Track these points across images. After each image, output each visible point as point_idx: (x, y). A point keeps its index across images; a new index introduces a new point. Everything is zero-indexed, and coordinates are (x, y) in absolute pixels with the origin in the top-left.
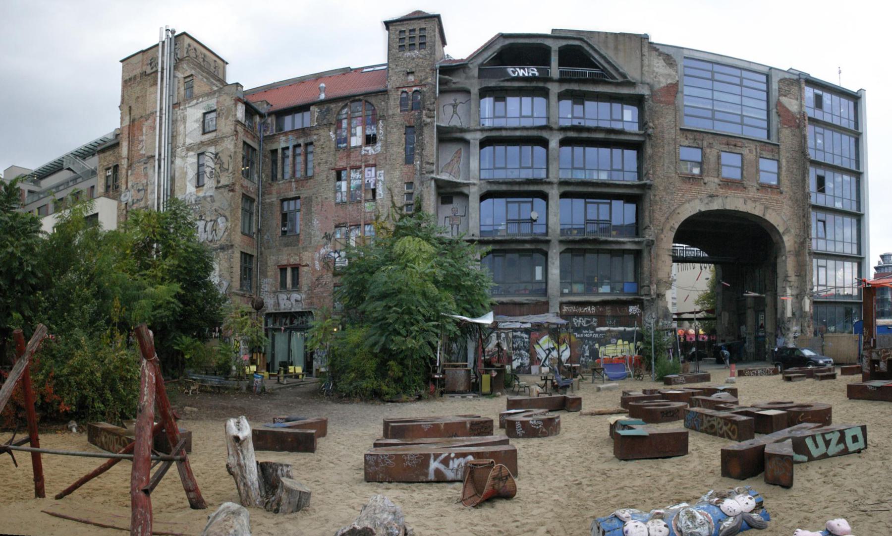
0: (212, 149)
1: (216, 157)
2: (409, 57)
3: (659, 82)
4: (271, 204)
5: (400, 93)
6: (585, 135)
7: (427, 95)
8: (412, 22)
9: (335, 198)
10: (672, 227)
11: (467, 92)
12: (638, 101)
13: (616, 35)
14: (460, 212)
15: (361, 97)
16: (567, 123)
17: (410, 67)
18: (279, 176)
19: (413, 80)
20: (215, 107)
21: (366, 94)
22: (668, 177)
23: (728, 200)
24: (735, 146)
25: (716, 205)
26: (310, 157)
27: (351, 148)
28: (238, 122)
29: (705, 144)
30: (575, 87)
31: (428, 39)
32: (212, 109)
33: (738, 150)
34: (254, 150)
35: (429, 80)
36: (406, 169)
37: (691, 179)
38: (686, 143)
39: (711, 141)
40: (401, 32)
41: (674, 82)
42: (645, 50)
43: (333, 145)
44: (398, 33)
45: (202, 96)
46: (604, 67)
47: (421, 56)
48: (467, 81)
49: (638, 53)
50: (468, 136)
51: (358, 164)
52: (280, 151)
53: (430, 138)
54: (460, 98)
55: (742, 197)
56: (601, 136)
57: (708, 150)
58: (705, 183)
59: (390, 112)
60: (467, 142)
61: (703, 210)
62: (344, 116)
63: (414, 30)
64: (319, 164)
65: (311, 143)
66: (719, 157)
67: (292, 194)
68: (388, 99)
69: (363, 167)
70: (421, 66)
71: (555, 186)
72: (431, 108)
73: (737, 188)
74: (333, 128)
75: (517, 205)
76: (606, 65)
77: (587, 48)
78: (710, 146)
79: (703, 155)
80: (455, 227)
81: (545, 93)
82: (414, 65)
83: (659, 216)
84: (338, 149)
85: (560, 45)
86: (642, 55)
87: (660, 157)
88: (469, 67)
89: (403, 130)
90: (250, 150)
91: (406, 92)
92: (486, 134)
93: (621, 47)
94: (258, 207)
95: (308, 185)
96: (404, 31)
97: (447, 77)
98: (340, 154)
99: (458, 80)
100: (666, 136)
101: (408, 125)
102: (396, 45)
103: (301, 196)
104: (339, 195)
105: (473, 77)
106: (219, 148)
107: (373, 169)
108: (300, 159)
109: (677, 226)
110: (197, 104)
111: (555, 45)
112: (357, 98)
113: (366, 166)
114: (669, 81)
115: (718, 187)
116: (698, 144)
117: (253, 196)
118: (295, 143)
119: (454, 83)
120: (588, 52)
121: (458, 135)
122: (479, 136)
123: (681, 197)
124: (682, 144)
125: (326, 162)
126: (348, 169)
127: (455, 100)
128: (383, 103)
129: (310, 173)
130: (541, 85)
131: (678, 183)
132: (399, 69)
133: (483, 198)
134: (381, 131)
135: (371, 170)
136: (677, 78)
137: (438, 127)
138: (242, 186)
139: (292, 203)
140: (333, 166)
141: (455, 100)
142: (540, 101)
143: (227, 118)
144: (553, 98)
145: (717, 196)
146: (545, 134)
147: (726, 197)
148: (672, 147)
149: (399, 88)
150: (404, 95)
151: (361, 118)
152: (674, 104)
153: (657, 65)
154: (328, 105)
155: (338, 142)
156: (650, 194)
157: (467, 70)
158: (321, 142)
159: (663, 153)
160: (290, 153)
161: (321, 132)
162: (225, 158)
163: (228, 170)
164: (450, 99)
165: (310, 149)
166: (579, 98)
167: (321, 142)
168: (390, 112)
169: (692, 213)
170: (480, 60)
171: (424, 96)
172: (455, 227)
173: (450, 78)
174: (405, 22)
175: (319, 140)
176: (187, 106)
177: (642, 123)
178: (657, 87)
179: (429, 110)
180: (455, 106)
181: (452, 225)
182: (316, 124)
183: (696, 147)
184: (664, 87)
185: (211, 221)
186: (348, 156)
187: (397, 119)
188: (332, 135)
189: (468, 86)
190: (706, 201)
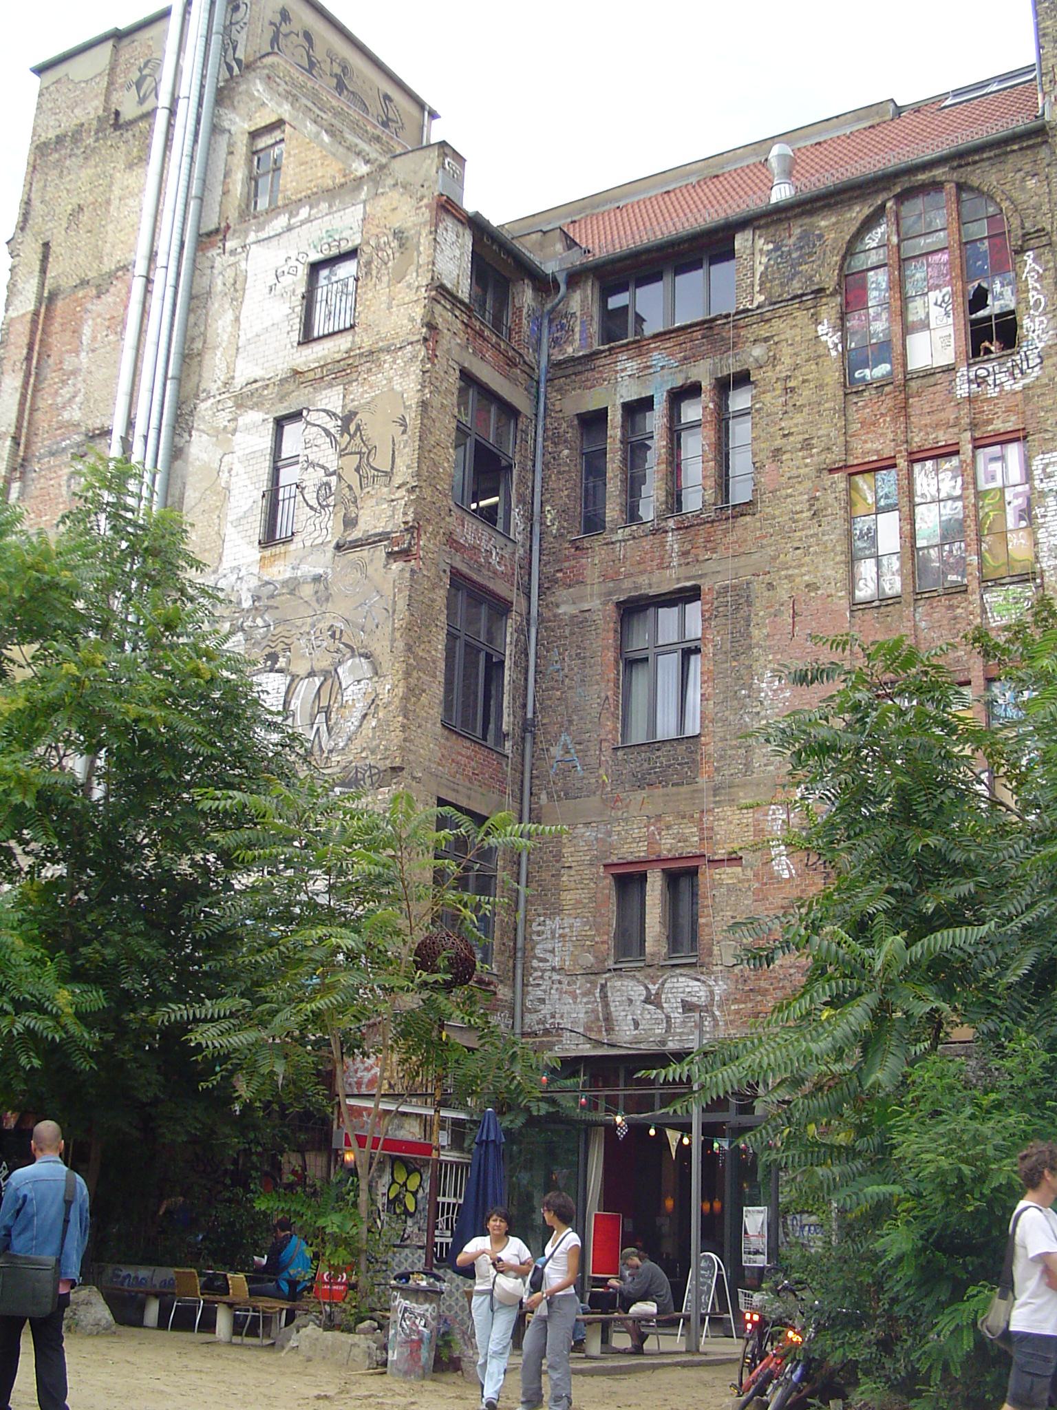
0: (332, 399)
1: (344, 429)
4: (581, 622)
9: (852, 581)
15: (939, 173)
18: (612, 511)
21: (961, 157)
26: (741, 431)
27: (908, 377)
28: (441, 292)
32: (346, 247)
34: (509, 412)
43: (833, 376)
45: (311, 199)
51: (943, 438)
52: (615, 418)
62: (874, 258)
65: (743, 379)
74: (829, 310)
84: (851, 388)
94: (523, 631)
95: (731, 538)
98: (863, 408)
103: (705, 588)
104: (867, 568)
106: (360, 394)
107: (1014, 452)
108: (695, 447)
110: (289, 229)
112: (922, 177)
113: (978, 445)
117: (500, 588)
118: (679, 382)
125: (807, 445)
126: (902, 463)
128: (1031, 183)
129: (740, 493)
134: (1033, 296)
135: (1002, 458)
138: (451, 541)
140: (836, 456)
151: (944, 257)
154: (807, 220)
155: (851, 361)
158: (782, 369)
160: (656, 421)
162: (379, 430)
163: (389, 474)
165: (740, 400)
167: (782, 369)
175: (774, 360)
176: (252, 237)
185: (311, 674)
186: (904, 409)
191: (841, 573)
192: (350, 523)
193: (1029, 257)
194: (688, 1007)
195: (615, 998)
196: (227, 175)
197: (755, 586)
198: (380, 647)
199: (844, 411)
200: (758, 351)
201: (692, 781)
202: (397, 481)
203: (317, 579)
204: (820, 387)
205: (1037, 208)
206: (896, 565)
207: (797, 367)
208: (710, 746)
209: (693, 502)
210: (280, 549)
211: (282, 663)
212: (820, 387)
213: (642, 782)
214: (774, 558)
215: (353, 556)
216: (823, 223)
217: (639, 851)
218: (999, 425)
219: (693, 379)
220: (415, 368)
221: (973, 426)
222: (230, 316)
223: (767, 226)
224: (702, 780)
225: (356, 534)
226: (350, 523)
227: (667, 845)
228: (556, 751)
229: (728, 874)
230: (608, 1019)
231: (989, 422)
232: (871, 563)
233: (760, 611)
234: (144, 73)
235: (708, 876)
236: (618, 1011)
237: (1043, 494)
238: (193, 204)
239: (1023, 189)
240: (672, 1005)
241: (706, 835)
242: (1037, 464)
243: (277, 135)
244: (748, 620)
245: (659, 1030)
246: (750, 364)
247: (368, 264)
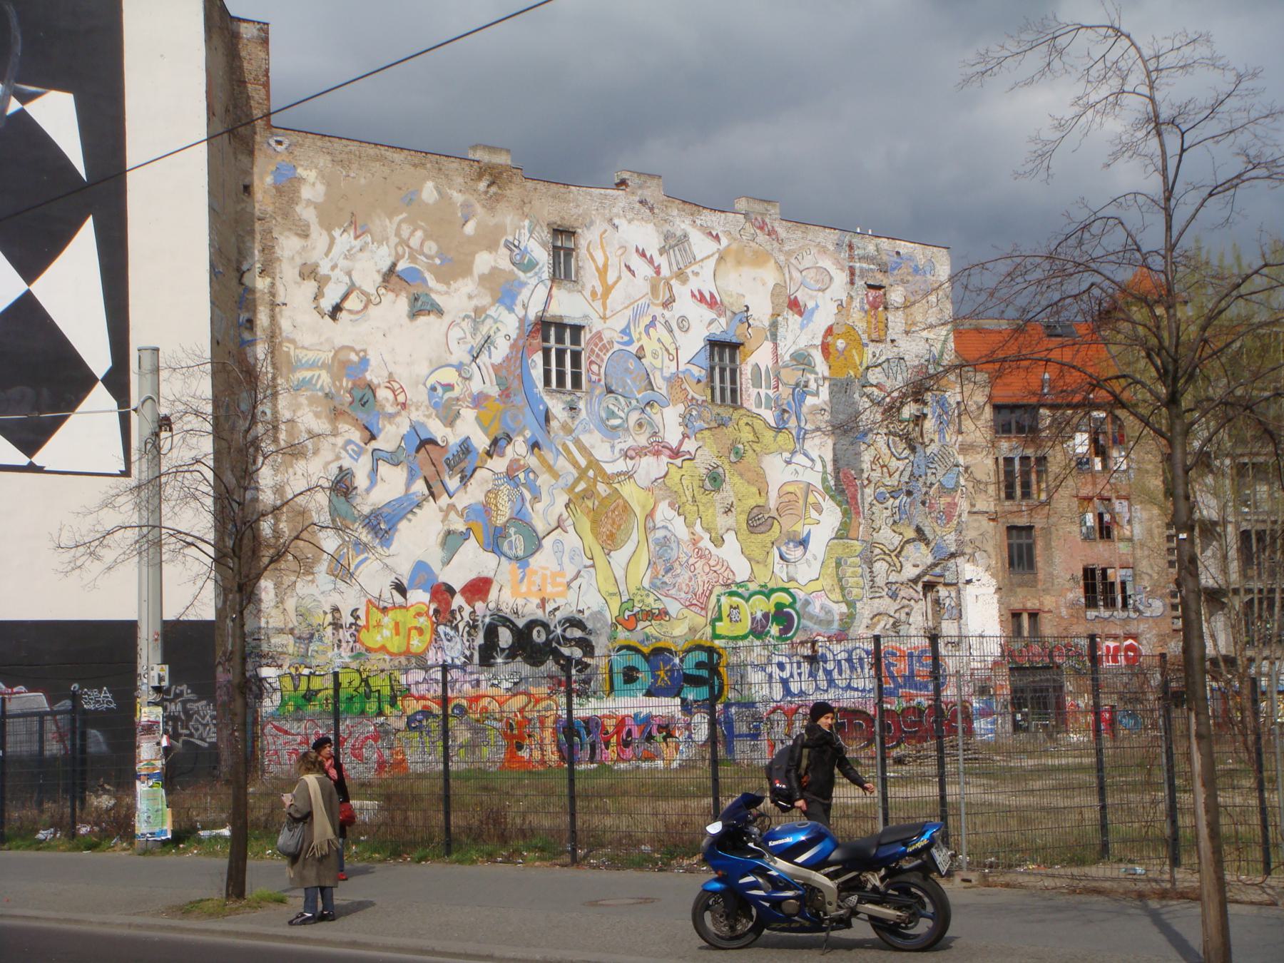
192: (973, 505)
198: (990, 549)
215: (975, 517)
224: (1039, 587)
225: (975, 510)
226: (973, 505)
227: (1029, 605)
233: (1054, 537)
235: (1042, 615)
241: (1042, 603)
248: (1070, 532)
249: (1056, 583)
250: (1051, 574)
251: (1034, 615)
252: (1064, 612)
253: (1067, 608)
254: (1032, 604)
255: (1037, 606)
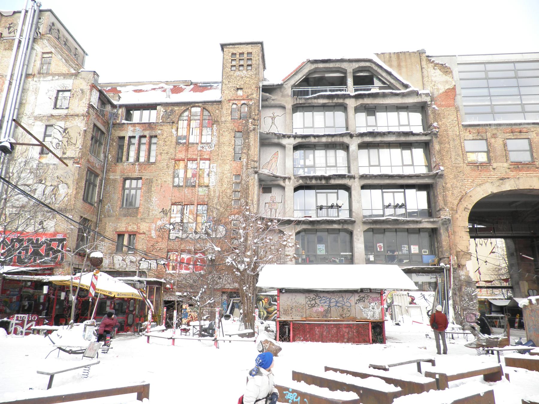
2: (239, 76)
3: (438, 89)
4: (115, 180)
5: (231, 105)
6: (378, 139)
7: (253, 107)
8: (242, 46)
9: (173, 182)
10: (465, 208)
11: (284, 107)
12: (422, 108)
13: (398, 54)
14: (278, 199)
15: (200, 104)
16: (363, 130)
17: (240, 84)
18: (124, 158)
19: (241, 95)
20: (70, 88)
22: (457, 167)
23: (521, 180)
24: (520, 132)
25: (508, 186)
26: (153, 147)
29: (489, 135)
30: (367, 101)
31: (254, 62)
33: (523, 135)
34: (103, 133)
35: (254, 96)
36: (234, 164)
37: (477, 166)
38: (471, 136)
39: (495, 132)
40: (233, 54)
41: (451, 87)
42: (424, 63)
44: (230, 54)
46: (390, 82)
47: (248, 76)
48: (283, 99)
49: (419, 67)
50: (284, 141)
51: (194, 157)
52: (127, 139)
53: (254, 141)
54: (278, 112)
55: (535, 176)
56: (392, 139)
57: (493, 140)
58: (494, 169)
59: (223, 119)
60: (283, 147)
61: (495, 191)
63: (243, 53)
64: (161, 154)
65: (156, 136)
66: (505, 145)
67: (136, 175)
68: (222, 109)
69: (199, 160)
70: (248, 84)
71: (357, 180)
72: (256, 118)
73: (528, 169)
75: (325, 194)
76: (392, 81)
77: (376, 68)
78: (494, 136)
79: (489, 145)
80: (273, 210)
81: (344, 108)
82: (243, 83)
83: (452, 200)
84: (178, 143)
85: (354, 68)
86: (422, 68)
87: (447, 151)
88: (284, 87)
89: (233, 134)
90: (99, 132)
91: (236, 104)
92: (299, 140)
93: (403, 64)
95: (150, 169)
96: (235, 54)
97: (267, 94)
98: (179, 148)
99: (276, 98)
100: (450, 133)
101: (237, 130)
102: (229, 65)
103: (143, 178)
105: (288, 96)
107: (208, 162)
108: (144, 148)
109: (470, 207)
110: (52, 80)
111: (350, 68)
112: (197, 104)
113: (201, 159)
114: (447, 87)
115: (508, 170)
116: (482, 136)
117: (98, 171)
118: (142, 134)
119: (273, 100)
120: (376, 71)
121: (276, 141)
122: (293, 142)
123: (472, 182)
124: (466, 138)
125: (167, 153)
126: (186, 160)
127: (273, 114)
128: (217, 111)
129: (152, 160)
130: (341, 101)
131: (467, 169)
132: (231, 85)
133: (296, 189)
136: (454, 84)
137: (261, 133)
139: (134, 182)
140: (173, 156)
141: (273, 114)
142: (340, 115)
143: (81, 99)
144: (351, 111)
145: (508, 178)
146: (346, 140)
147: (518, 178)
148: (457, 142)
149: (230, 100)
150: (234, 106)
151: (199, 121)
152: (454, 105)
153: (434, 75)
154: (172, 107)
156: (440, 183)
157: (283, 90)
158: (164, 137)
159: (450, 148)
161: (164, 128)
164: (269, 112)
165: (154, 140)
166: (371, 110)
167: (164, 137)
168: (223, 119)
169: (485, 196)
170: (293, 82)
171: (250, 108)
172: (273, 210)
173: (271, 96)
174: (236, 46)
176: (41, 79)
177: (426, 124)
178: (436, 94)
179: (254, 119)
180: (273, 118)
181: (271, 209)
182: (161, 121)
183: (480, 139)
184: (443, 93)
186: (187, 150)
187: (228, 125)
188: (174, 131)
189: (283, 103)
190: (498, 184)
191: (171, 180)
193: (215, 125)
194: (131, 262)
195: (115, 259)
196: (35, 61)
197: (154, 179)
198: (70, 182)
199: (175, 148)
200: (159, 132)
201: (136, 217)
202: (77, 146)
203: (54, 164)
204: (171, 142)
205: (218, 116)
206: (182, 180)
207: (167, 137)
208: (141, 210)
209: (142, 159)
210: (45, 155)
211: (43, 182)
212: (171, 142)
213: (125, 216)
214: (158, 174)
216: (176, 109)
217: (124, 229)
218: (205, 157)
219: (145, 134)
220: (84, 122)
221: (200, 156)
222: (34, 97)
223: (164, 106)
224: (139, 217)
227: (130, 229)
228: (106, 207)
229: (142, 236)
230: (113, 263)
231: (204, 156)
232: (178, 178)
233: (154, 184)
234: (11, 26)
235: (138, 235)
236: (116, 261)
237: (212, 172)
238: (25, 66)
239: (216, 112)
240: (128, 261)
241: (138, 228)
242: (211, 166)
243: (50, 55)
244: (151, 186)
245: (125, 266)
246: (157, 134)
247: (73, 94)
248: (165, 181)
249: (151, 214)
250: (148, 208)
251: (133, 235)
252: (154, 234)
253: (156, 231)
254: (132, 228)
255: (135, 229)
